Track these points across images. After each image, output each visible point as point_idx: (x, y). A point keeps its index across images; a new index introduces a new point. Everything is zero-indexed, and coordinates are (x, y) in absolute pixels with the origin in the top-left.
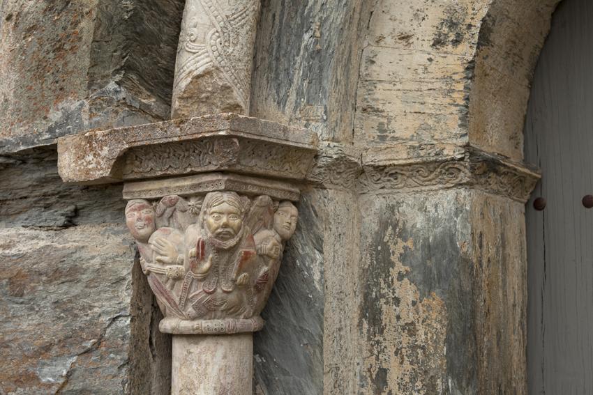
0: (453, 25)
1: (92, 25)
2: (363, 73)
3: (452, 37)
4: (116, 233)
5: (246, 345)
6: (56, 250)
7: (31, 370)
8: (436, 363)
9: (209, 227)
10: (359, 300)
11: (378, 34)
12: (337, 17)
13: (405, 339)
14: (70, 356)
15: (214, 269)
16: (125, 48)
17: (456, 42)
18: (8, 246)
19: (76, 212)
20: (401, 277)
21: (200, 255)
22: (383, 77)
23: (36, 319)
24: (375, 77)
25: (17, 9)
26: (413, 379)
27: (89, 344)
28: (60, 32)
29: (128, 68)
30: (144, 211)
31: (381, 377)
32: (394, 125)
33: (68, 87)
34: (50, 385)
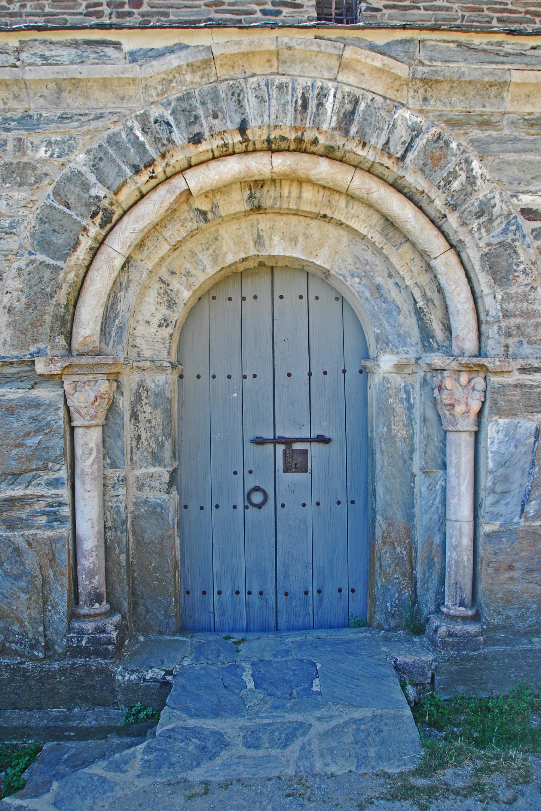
0: (165, 320)
1: (50, 318)
2: (131, 332)
3: (165, 324)
4: (54, 392)
5: (101, 428)
6: (28, 398)
7: (22, 442)
8: (159, 432)
9: (100, 391)
10: (130, 411)
11: (137, 319)
12: (127, 315)
13: (148, 425)
14: (39, 435)
15: (99, 404)
16: (61, 326)
17: (166, 327)
18: (3, 396)
19: (36, 383)
20: (146, 404)
21: (96, 400)
22: (139, 335)
23: (21, 423)
24: (136, 335)
25: (9, 304)
26: (151, 438)
27: (48, 431)
28: (34, 318)
29: (62, 333)
30: (72, 385)
31: (139, 438)
32: (143, 352)
33: (39, 339)
34: (31, 447)
